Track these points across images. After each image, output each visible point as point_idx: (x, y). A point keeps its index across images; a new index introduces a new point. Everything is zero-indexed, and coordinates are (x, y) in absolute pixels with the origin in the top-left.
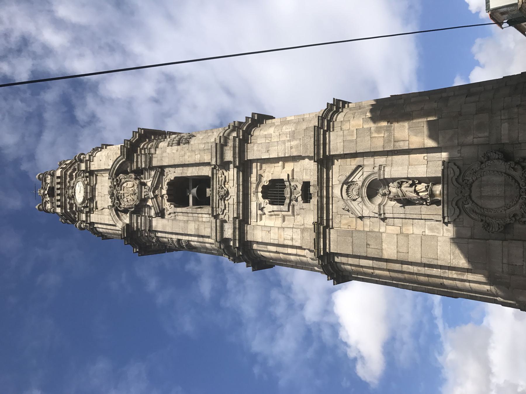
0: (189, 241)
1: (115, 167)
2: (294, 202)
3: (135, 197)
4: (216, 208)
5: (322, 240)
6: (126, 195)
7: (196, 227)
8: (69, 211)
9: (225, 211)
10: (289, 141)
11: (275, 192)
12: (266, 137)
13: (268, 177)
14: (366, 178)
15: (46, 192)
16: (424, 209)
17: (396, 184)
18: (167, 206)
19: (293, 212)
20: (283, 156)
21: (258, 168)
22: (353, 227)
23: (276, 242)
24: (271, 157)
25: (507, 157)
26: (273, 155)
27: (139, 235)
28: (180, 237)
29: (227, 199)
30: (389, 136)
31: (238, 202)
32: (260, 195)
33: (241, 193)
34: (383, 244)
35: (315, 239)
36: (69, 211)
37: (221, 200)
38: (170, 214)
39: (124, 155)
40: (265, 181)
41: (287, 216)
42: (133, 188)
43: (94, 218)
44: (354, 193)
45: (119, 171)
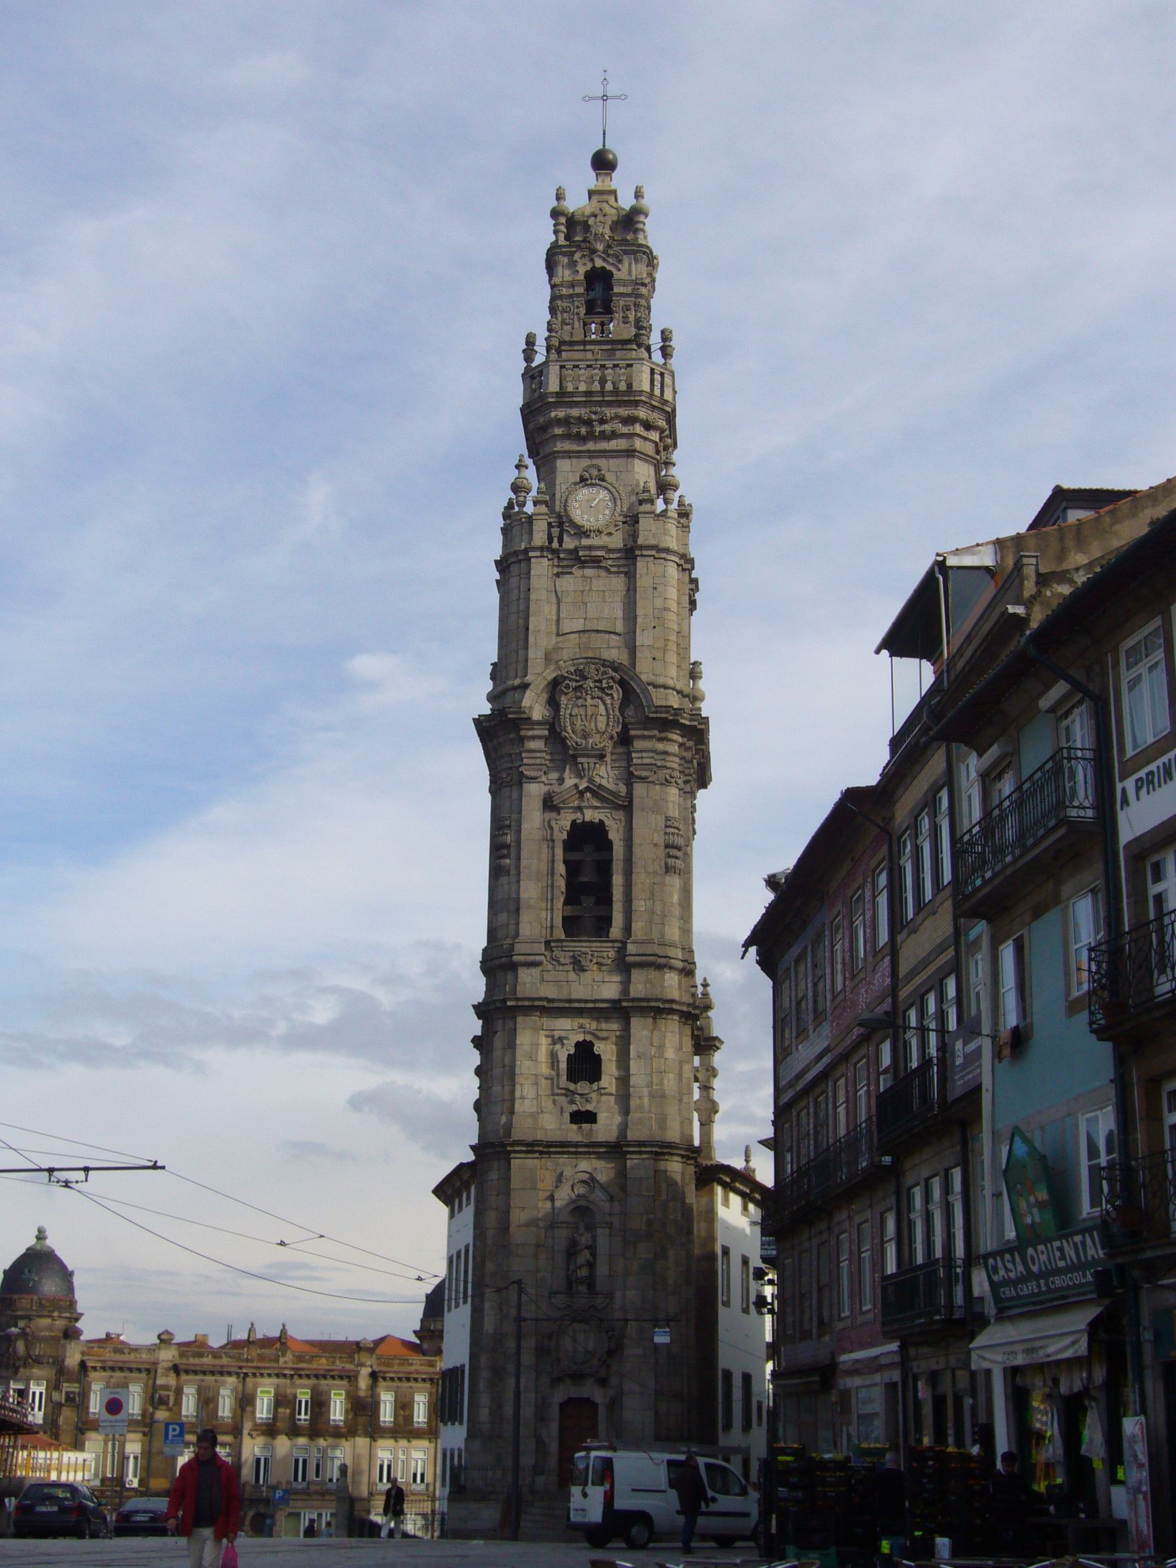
7: (532, 902)
8: (553, 414)
11: (584, 1065)
12: (661, 1047)
15: (599, 263)
17: (590, 1243)
18: (565, 821)
20: (632, 1083)
22: (540, 1185)
24: (632, 1062)
25: (611, 1353)
26: (634, 1067)
27: (512, 736)
28: (513, 850)
31: (570, 1001)
32: (581, 1038)
33: (583, 1005)
36: (553, 414)
37: (574, 957)
39: (656, 712)
40: (599, 1048)
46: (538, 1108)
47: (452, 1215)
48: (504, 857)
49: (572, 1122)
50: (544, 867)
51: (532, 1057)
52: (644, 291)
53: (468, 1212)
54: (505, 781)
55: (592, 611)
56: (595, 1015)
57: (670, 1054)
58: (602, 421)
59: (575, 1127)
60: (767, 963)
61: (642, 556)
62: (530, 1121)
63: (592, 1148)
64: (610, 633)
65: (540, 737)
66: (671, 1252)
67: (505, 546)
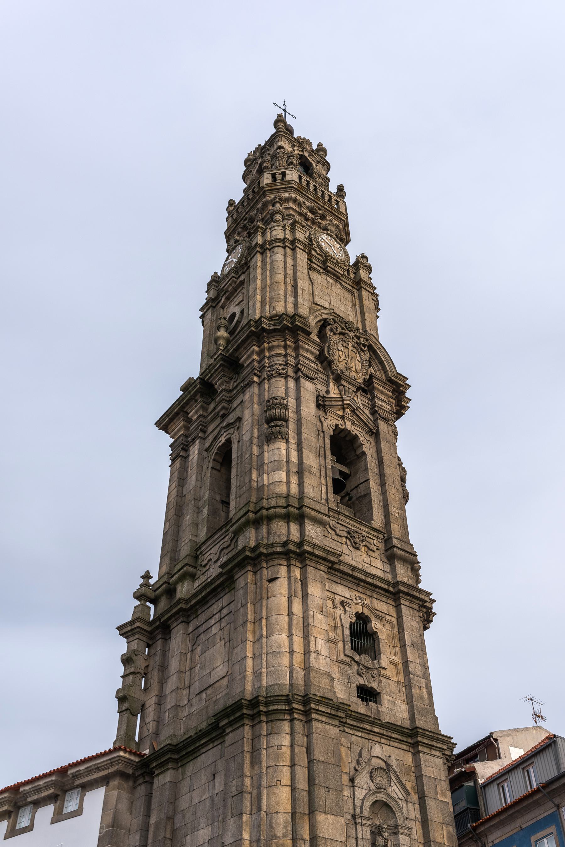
0: (287, 441)
1: (381, 351)
2: (355, 667)
3: (342, 366)
4: (338, 519)
5: (329, 711)
6: (346, 350)
7: (314, 470)
9: (333, 533)
14: (398, 804)
15: (306, 154)
19: (342, 662)
21: (388, 618)
24: (408, 648)
28: (292, 426)
29: (348, 542)
31: (354, 568)
33: (363, 577)
34: (332, 817)
35: (332, 700)
36: (293, 196)
37: (349, 533)
38: (321, 422)
39: (396, 377)
40: (376, 625)
41: (337, 648)
42: (354, 369)
44: (380, 779)
48: (282, 426)
56: (369, 593)
58: (323, 217)
61: (365, 289)
62: (325, 683)
65: (312, 353)
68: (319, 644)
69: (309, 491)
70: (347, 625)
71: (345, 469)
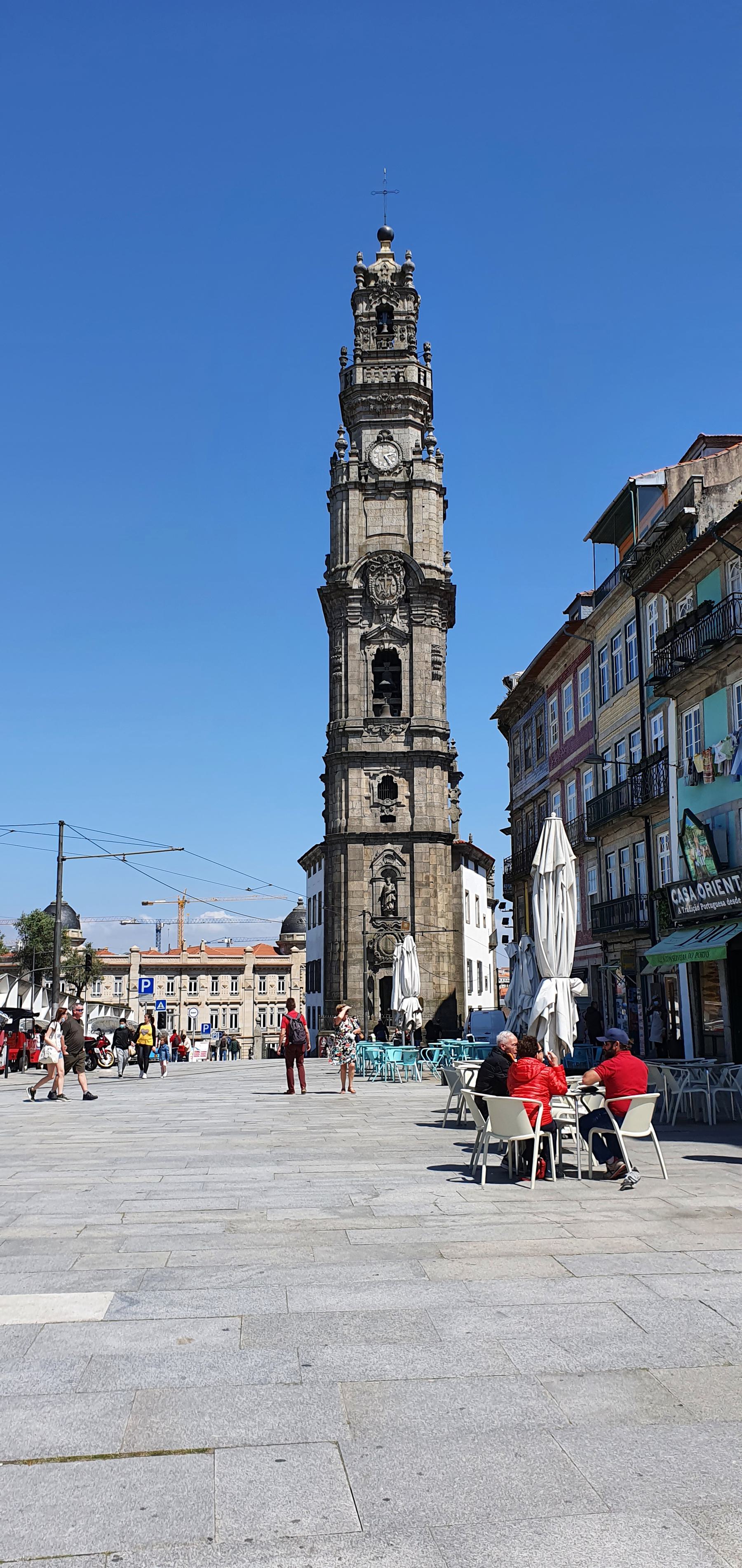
6: (382, 583)
7: (356, 697)
10: (426, 805)
11: (388, 789)
12: (432, 778)
13: (400, 782)
15: (384, 301)
16: (378, 906)
18: (373, 649)
23: (350, 793)
28: (343, 666)
30: (423, 885)
31: (379, 753)
32: (385, 774)
40: (396, 779)
43: (355, 496)
45: (407, 565)
46: (361, 814)
47: (309, 876)
49: (382, 821)
50: (362, 676)
51: (358, 785)
52: (412, 318)
53: (321, 874)
54: (337, 626)
55: (386, 522)
57: (436, 782)
59: (383, 824)
60: (504, 729)
63: (394, 838)
64: (397, 535)
66: (439, 894)
67: (332, 482)
68: (354, 804)
69: (351, 712)
70: (376, 786)
71: (394, 669)
